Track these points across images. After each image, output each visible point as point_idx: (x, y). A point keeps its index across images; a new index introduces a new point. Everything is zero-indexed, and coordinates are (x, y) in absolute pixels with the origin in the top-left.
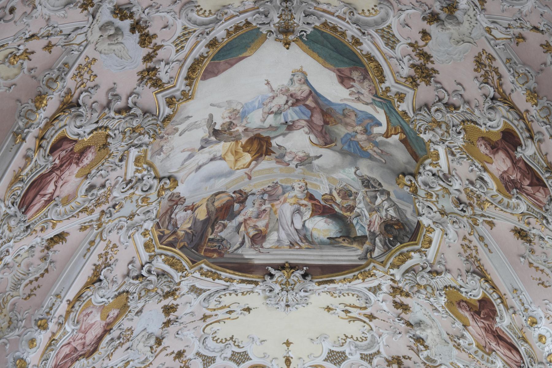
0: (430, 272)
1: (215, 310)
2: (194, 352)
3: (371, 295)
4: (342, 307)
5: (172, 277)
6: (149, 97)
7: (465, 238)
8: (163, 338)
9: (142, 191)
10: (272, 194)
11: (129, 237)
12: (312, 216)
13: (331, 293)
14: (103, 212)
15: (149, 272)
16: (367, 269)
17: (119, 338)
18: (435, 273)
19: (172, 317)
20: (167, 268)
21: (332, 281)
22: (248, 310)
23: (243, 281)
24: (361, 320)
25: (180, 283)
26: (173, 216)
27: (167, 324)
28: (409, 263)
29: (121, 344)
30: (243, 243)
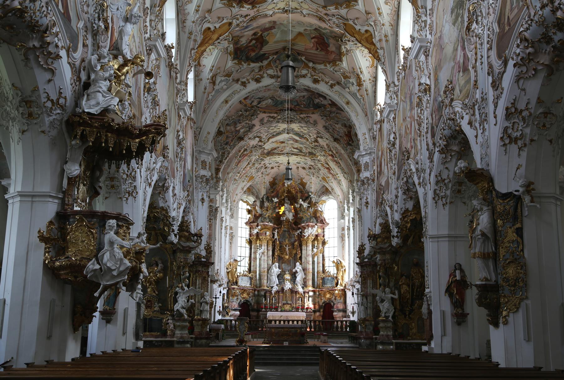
6: (260, 144)
10: (285, 147)
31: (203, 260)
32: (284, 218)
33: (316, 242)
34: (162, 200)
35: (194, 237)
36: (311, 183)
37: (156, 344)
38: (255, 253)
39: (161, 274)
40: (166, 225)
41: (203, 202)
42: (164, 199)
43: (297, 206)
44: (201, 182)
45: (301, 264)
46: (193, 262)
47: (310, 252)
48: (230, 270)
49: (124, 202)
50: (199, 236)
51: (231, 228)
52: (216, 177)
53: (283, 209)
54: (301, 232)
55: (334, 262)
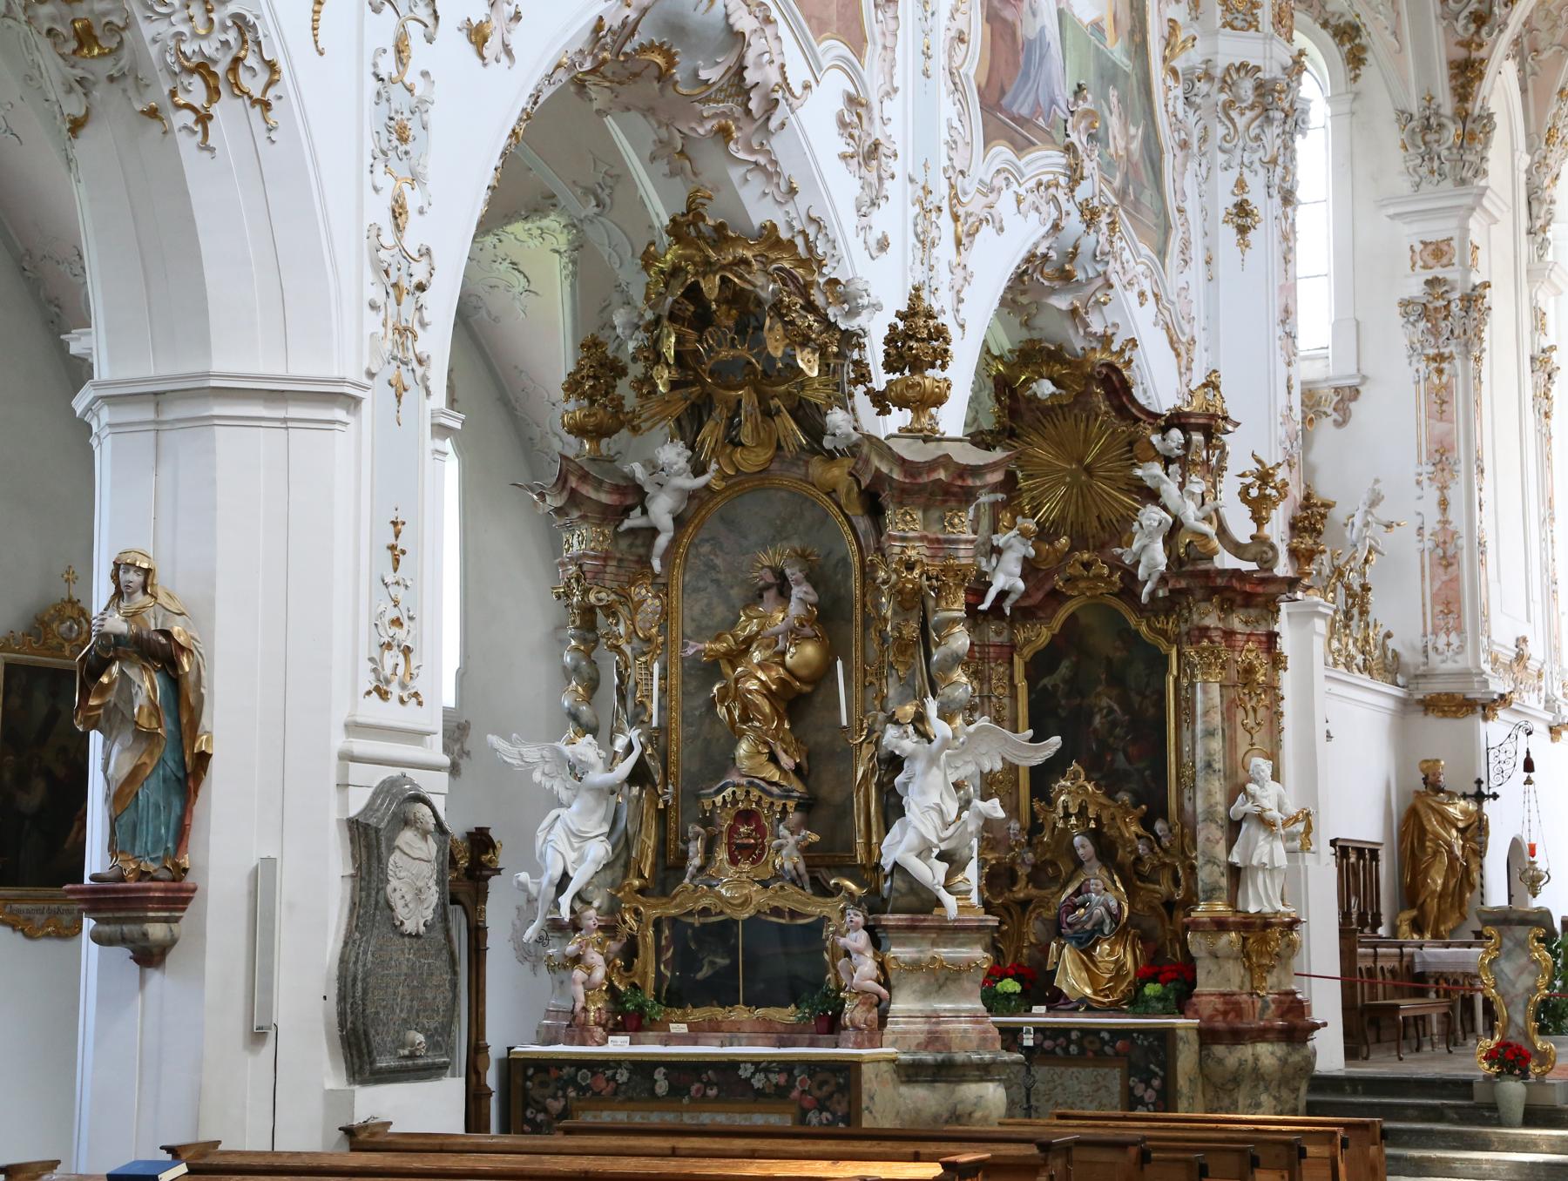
31: (1226, 561)
34: (756, 180)
35: (1164, 430)
37: (758, 1082)
39: (810, 651)
40: (805, 342)
41: (1243, 230)
42: (769, 171)
44: (1228, 106)
46: (1163, 580)
49: (187, 144)
50: (1204, 426)
52: (1463, 116)
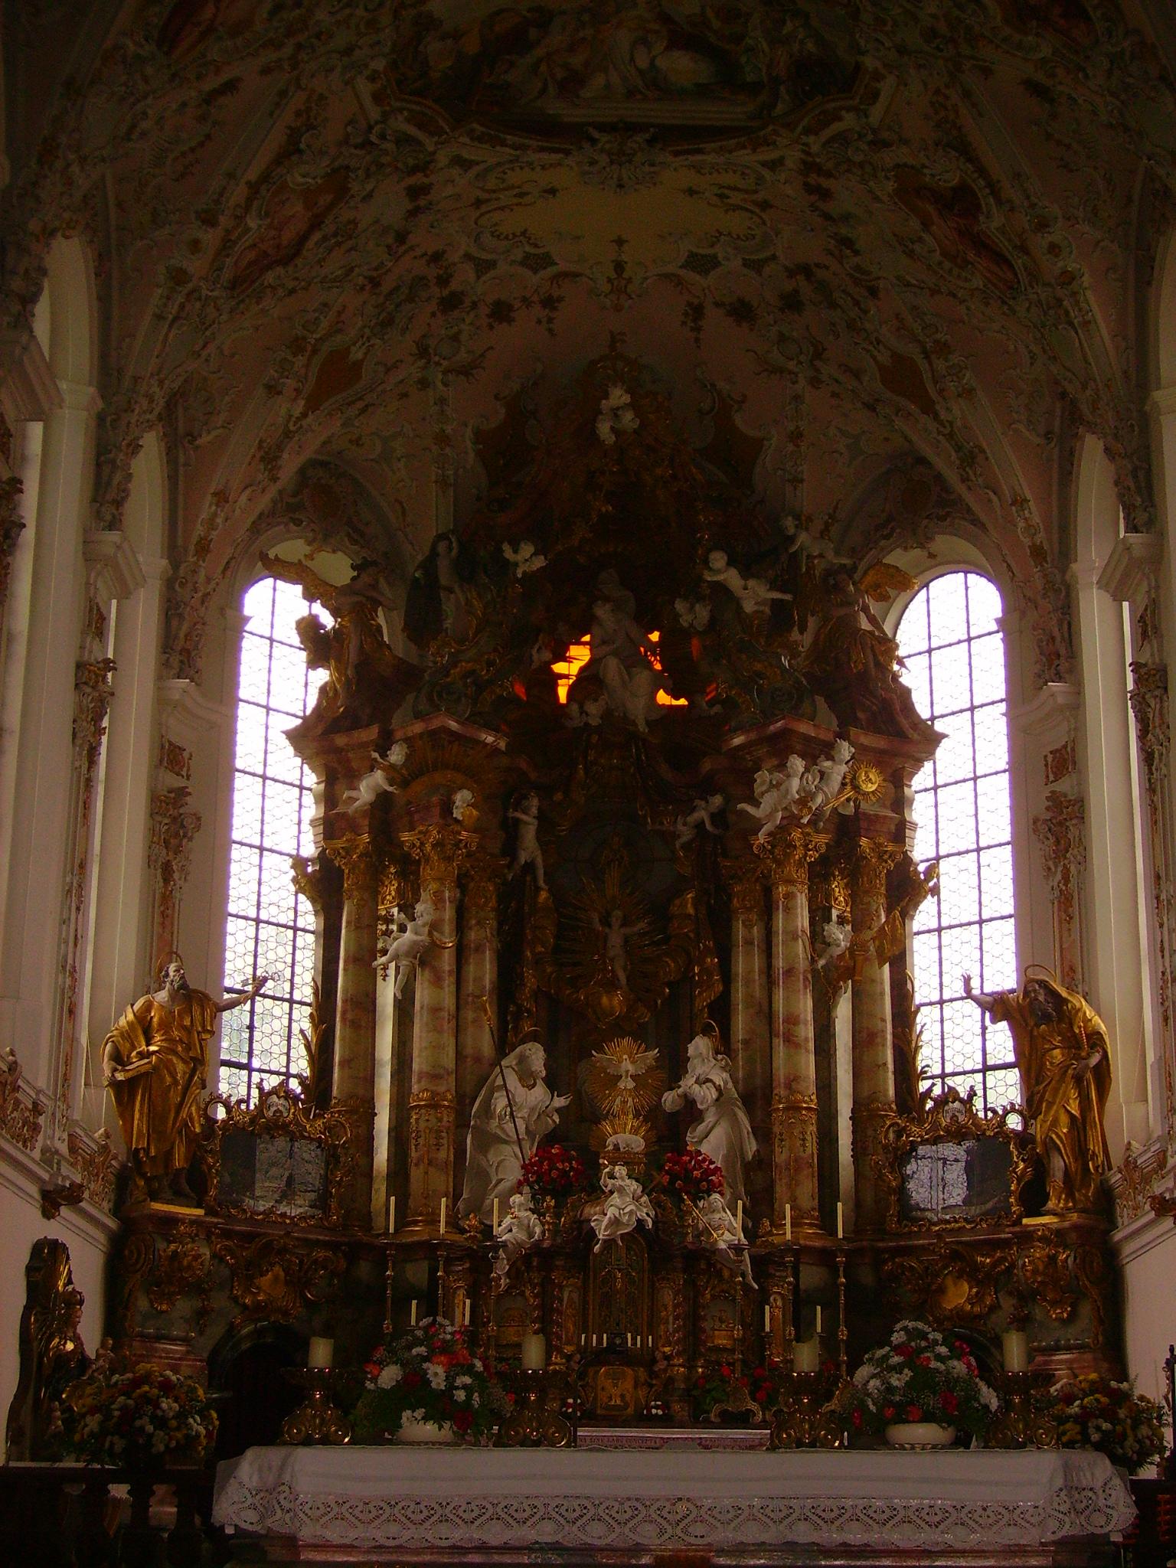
0: (872, 143)
1: (494, 191)
2: (461, 252)
3: (767, 174)
4: (716, 190)
5: (419, 143)
7: (937, 92)
8: (409, 233)
9: (366, 9)
11: (347, 83)
12: (668, 48)
13: (697, 168)
14: (299, 47)
15: (383, 137)
16: (762, 133)
17: (335, 235)
18: (879, 144)
19: (422, 202)
20: (412, 130)
21: (700, 151)
22: (553, 192)
23: (542, 150)
24: (747, 210)
25: (434, 153)
26: (421, 48)
27: (413, 213)
28: (836, 127)
29: (339, 244)
30: (544, 91)
32: (594, 709)
33: (839, 890)
36: (796, 437)
38: (365, 961)
43: (693, 615)
45: (724, 1047)
47: (801, 949)
48: (137, 1064)
51: (170, 757)
53: (581, 654)
54: (719, 817)
55: (996, 1006)
